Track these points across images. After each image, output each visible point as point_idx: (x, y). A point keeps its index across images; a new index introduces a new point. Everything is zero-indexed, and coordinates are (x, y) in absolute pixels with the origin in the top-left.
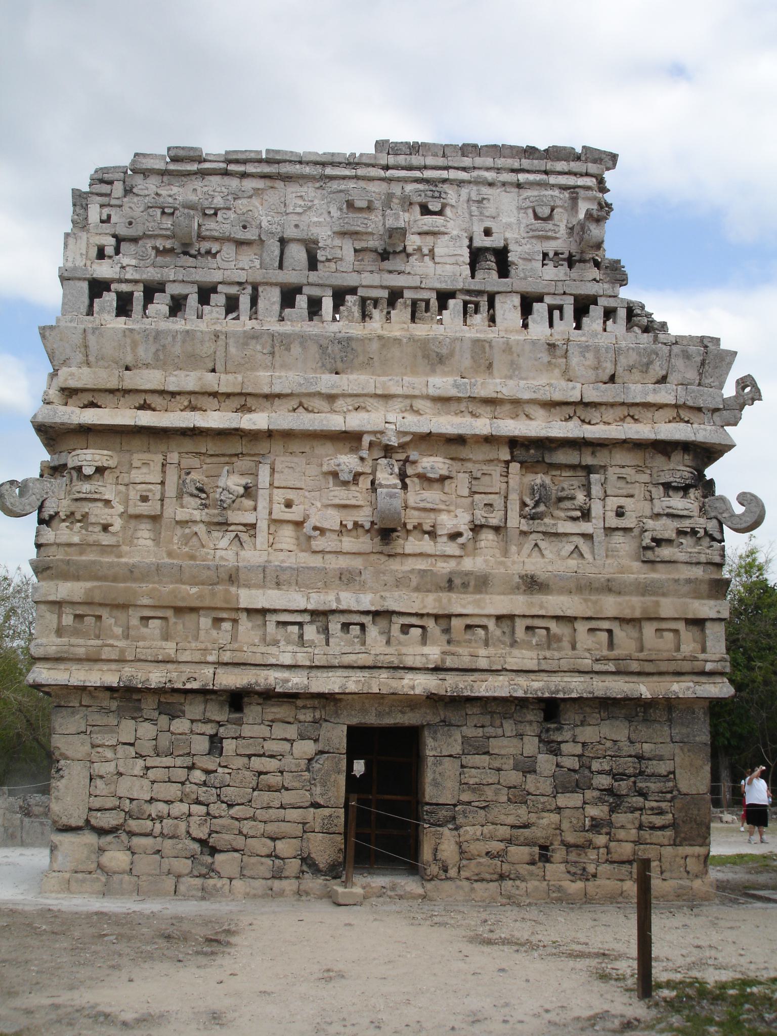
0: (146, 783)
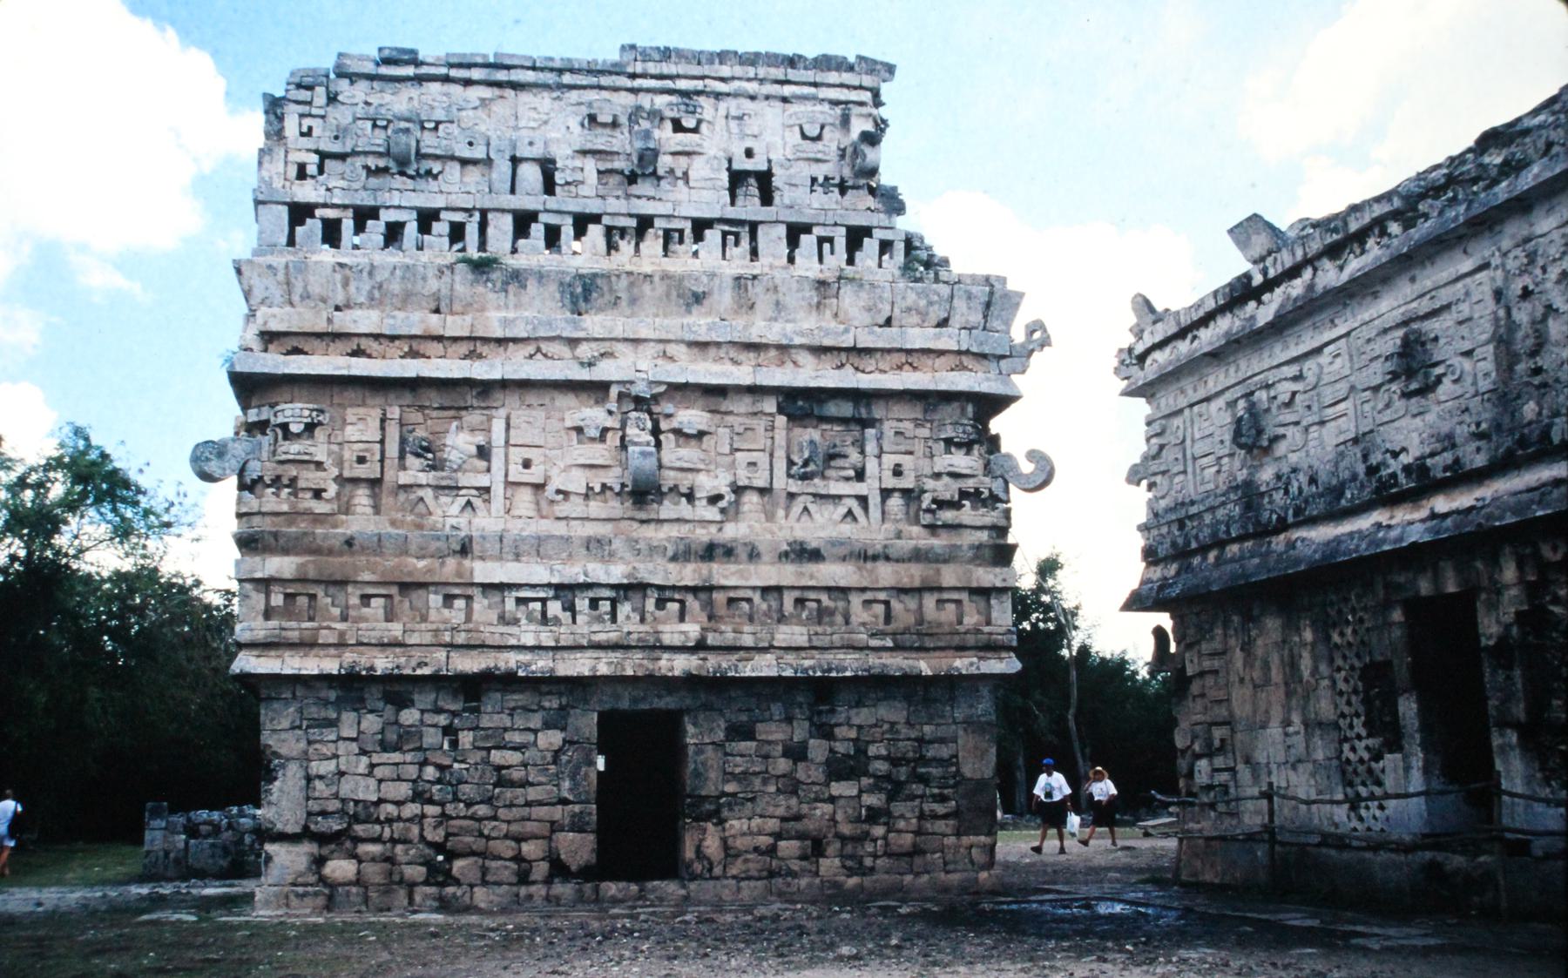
0: (372, 782)
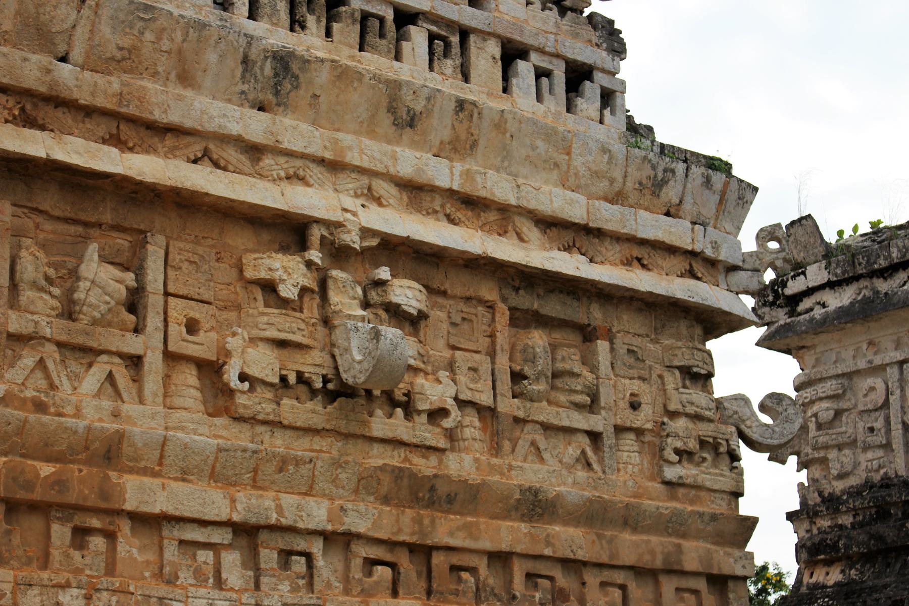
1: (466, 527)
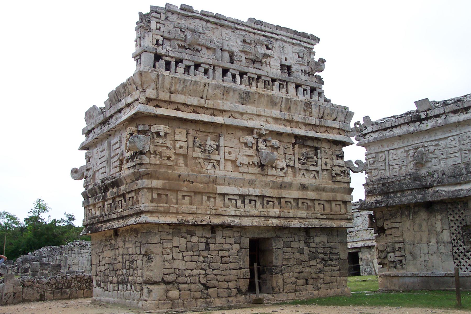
0: (184, 262)
1: (289, 193)
